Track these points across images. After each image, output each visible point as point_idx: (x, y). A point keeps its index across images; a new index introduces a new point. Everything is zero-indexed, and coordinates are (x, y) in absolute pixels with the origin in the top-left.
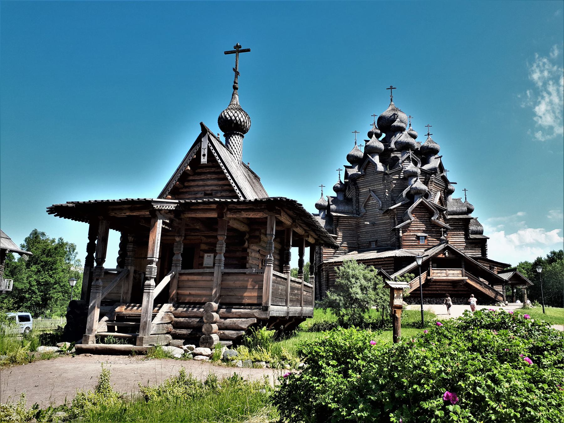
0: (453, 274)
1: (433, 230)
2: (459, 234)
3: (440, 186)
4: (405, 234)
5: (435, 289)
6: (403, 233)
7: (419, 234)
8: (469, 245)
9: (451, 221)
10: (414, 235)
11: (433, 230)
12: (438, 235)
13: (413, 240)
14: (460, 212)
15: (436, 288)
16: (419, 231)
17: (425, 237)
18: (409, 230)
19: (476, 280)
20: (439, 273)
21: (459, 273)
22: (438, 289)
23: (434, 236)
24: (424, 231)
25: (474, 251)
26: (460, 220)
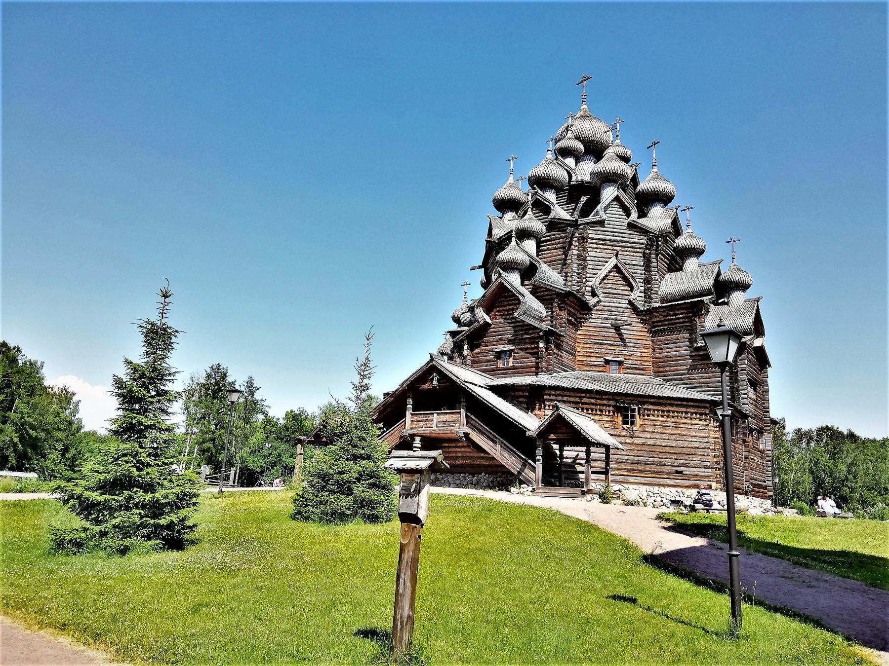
0: (445, 422)
1: (525, 336)
2: (678, 339)
3: (620, 244)
4: (477, 350)
5: (454, 455)
6: (471, 349)
7: (500, 348)
8: (700, 363)
9: (658, 314)
10: (492, 350)
11: (525, 336)
12: (533, 346)
13: (489, 361)
14: (697, 292)
15: (457, 452)
16: (501, 342)
17: (511, 351)
18: (483, 342)
19: (487, 433)
20: (421, 421)
21: (455, 419)
22: (459, 455)
23: (527, 349)
24: (510, 342)
25: (711, 375)
26: (678, 310)
